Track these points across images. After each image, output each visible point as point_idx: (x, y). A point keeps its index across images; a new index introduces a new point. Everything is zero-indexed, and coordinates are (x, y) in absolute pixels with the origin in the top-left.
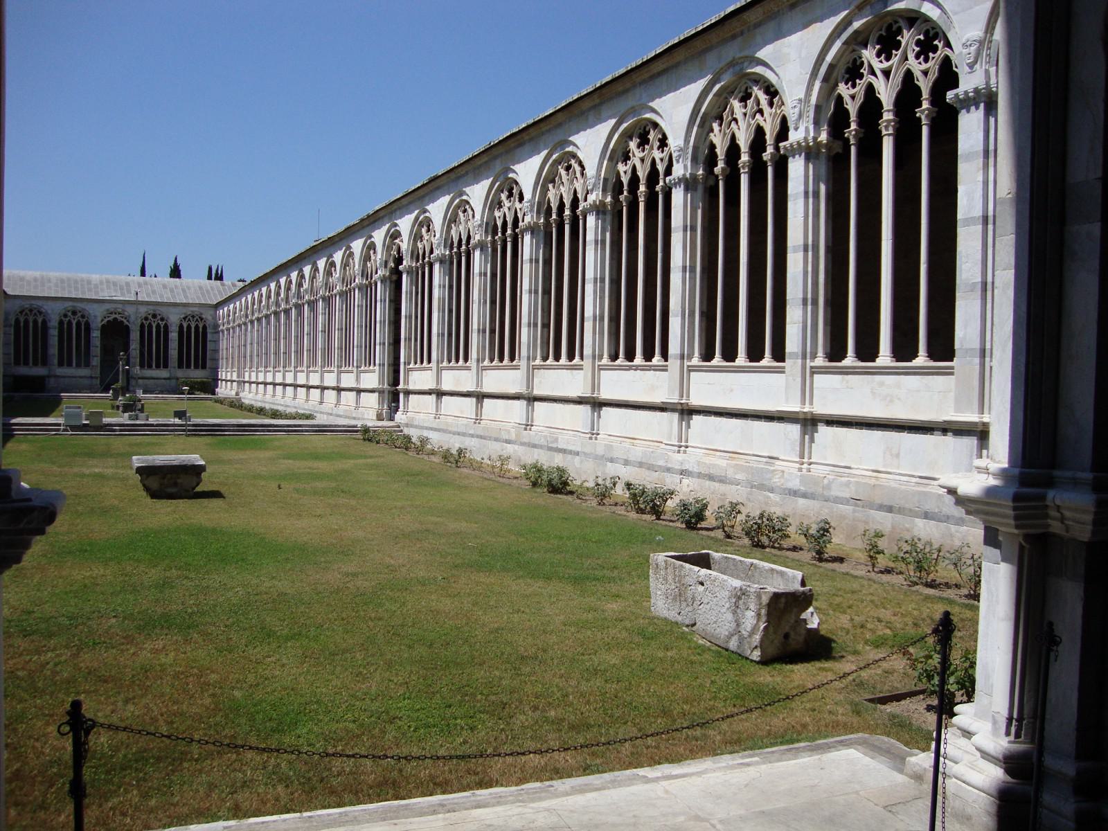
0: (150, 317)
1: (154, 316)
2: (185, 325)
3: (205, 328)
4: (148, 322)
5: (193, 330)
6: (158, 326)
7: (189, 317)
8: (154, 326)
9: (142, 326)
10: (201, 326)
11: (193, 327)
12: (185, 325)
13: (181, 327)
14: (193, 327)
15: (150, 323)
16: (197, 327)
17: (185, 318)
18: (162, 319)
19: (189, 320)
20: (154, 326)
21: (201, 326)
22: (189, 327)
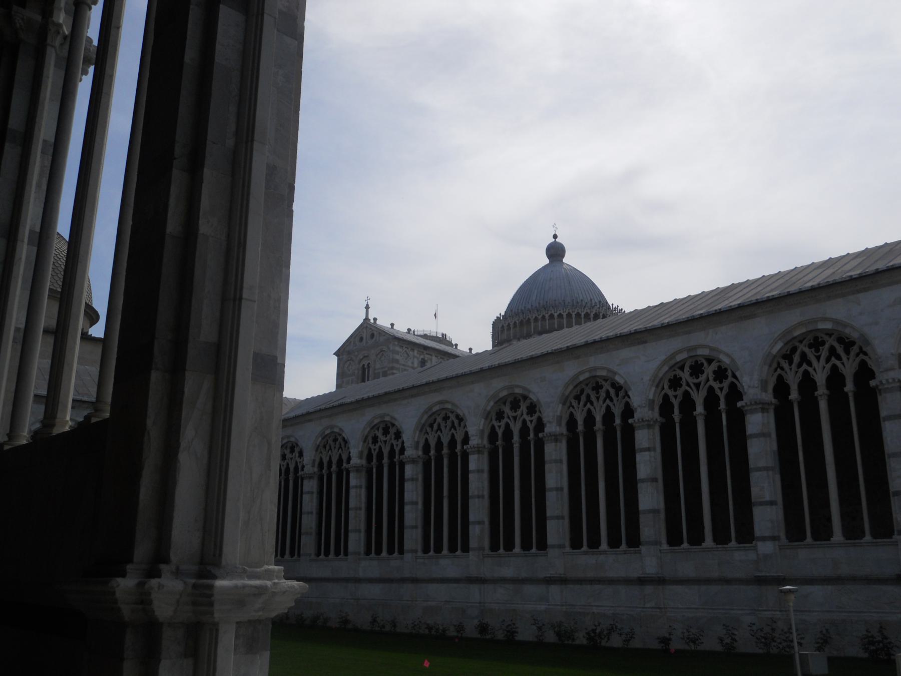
0: (685, 375)
1: (697, 369)
2: (793, 380)
3: (865, 373)
4: (680, 392)
5: (822, 390)
6: (711, 400)
7: (803, 348)
8: (699, 399)
9: (666, 407)
10: (848, 369)
11: (820, 377)
12: (793, 380)
13: (781, 388)
14: (820, 377)
15: (686, 394)
16: (835, 379)
17: (788, 357)
18: (721, 374)
19: (804, 358)
20: (699, 399)
21: (848, 369)
22: (807, 384)
